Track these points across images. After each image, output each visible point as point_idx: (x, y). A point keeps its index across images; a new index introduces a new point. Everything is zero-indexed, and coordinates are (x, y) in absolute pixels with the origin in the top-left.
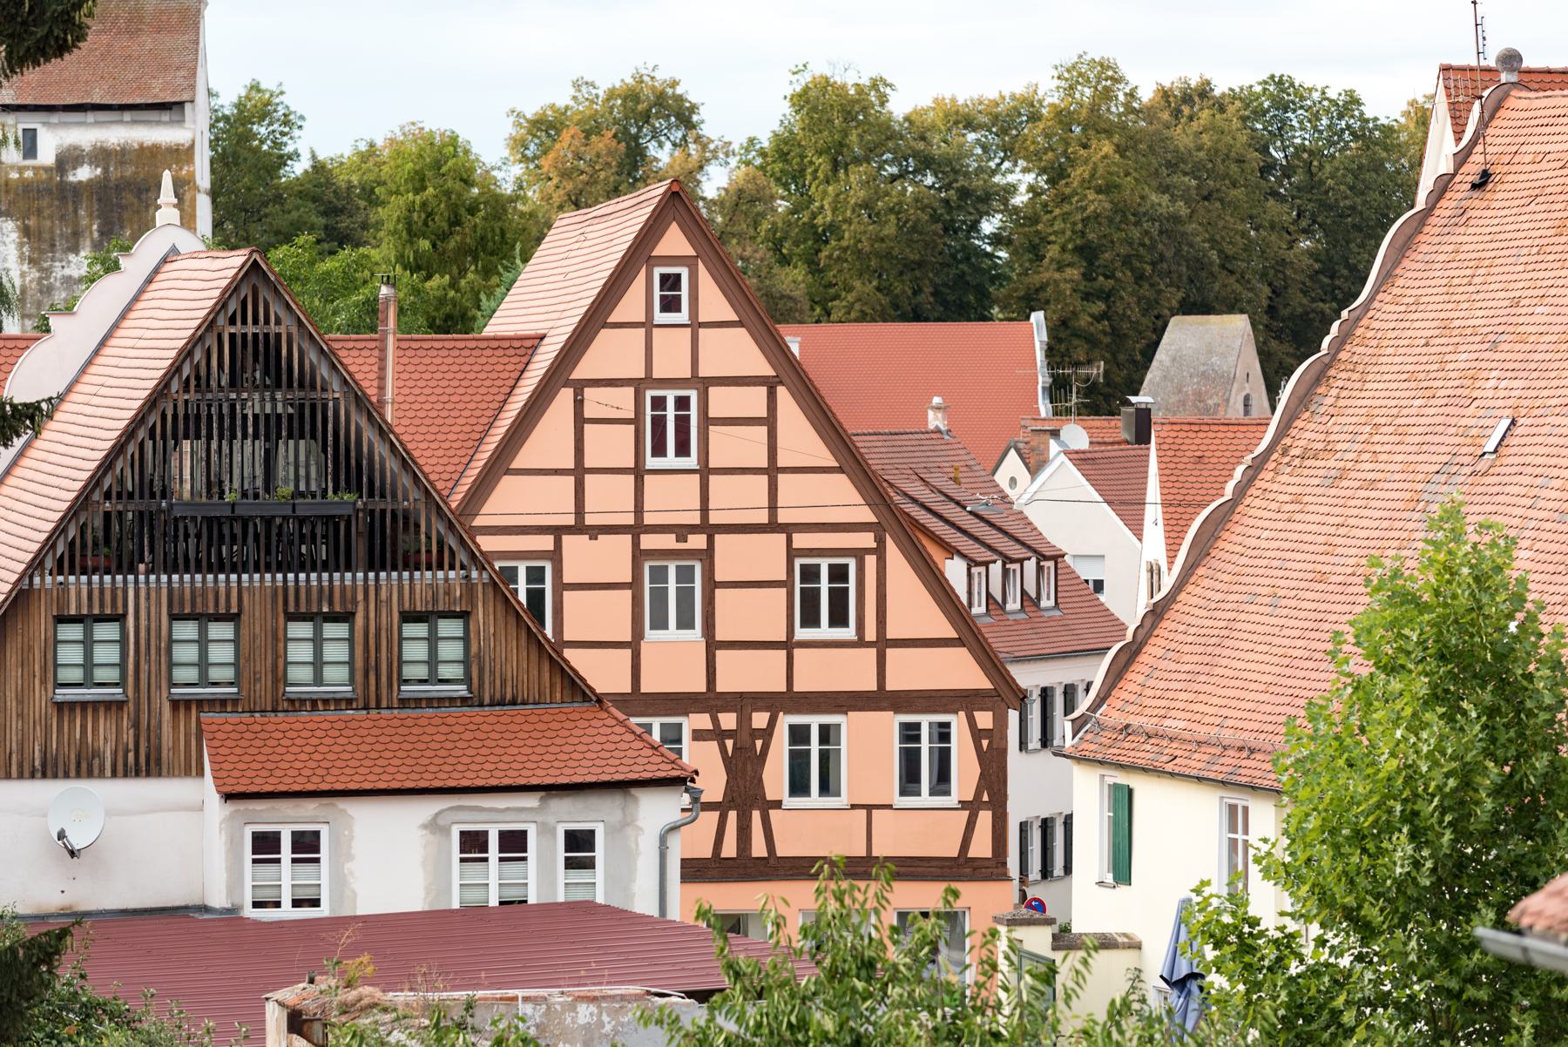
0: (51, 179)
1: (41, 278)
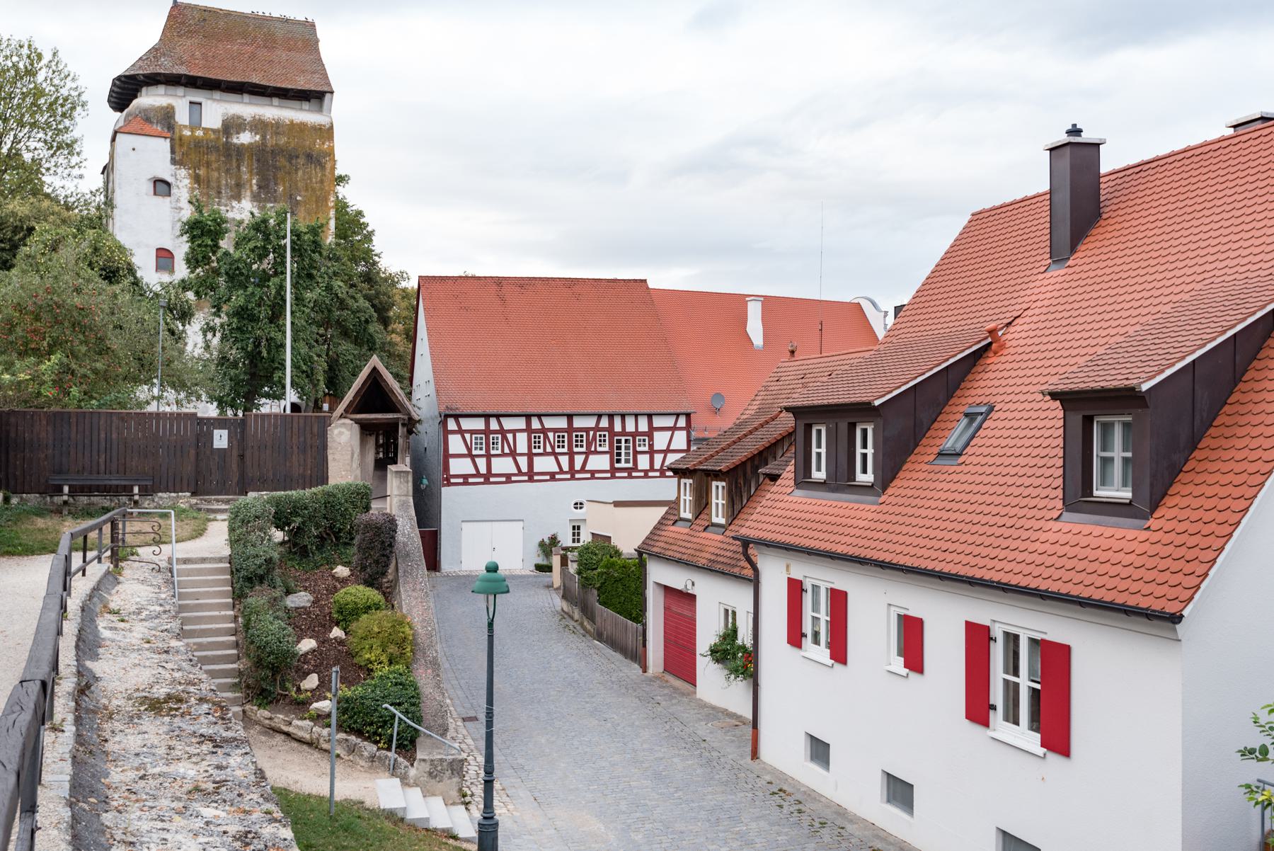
0: (218, 138)
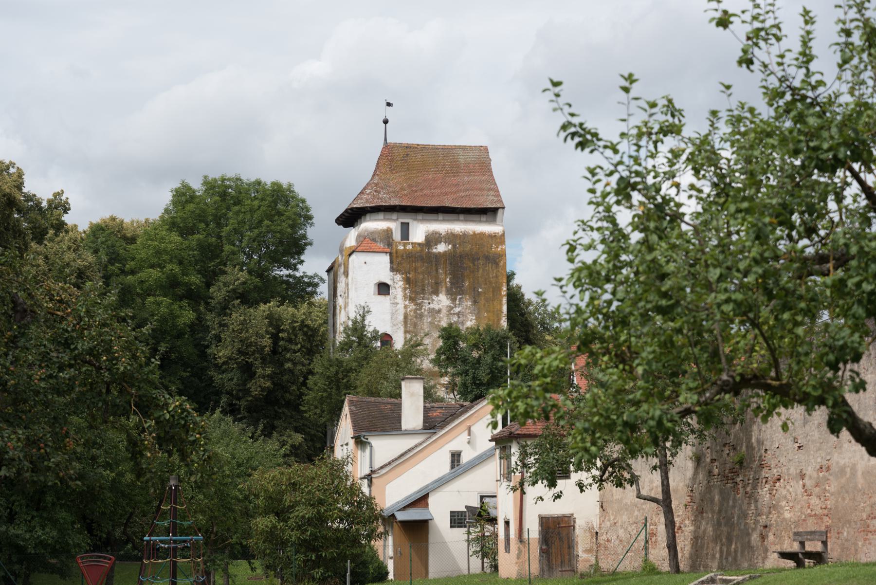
1: (416, 309)
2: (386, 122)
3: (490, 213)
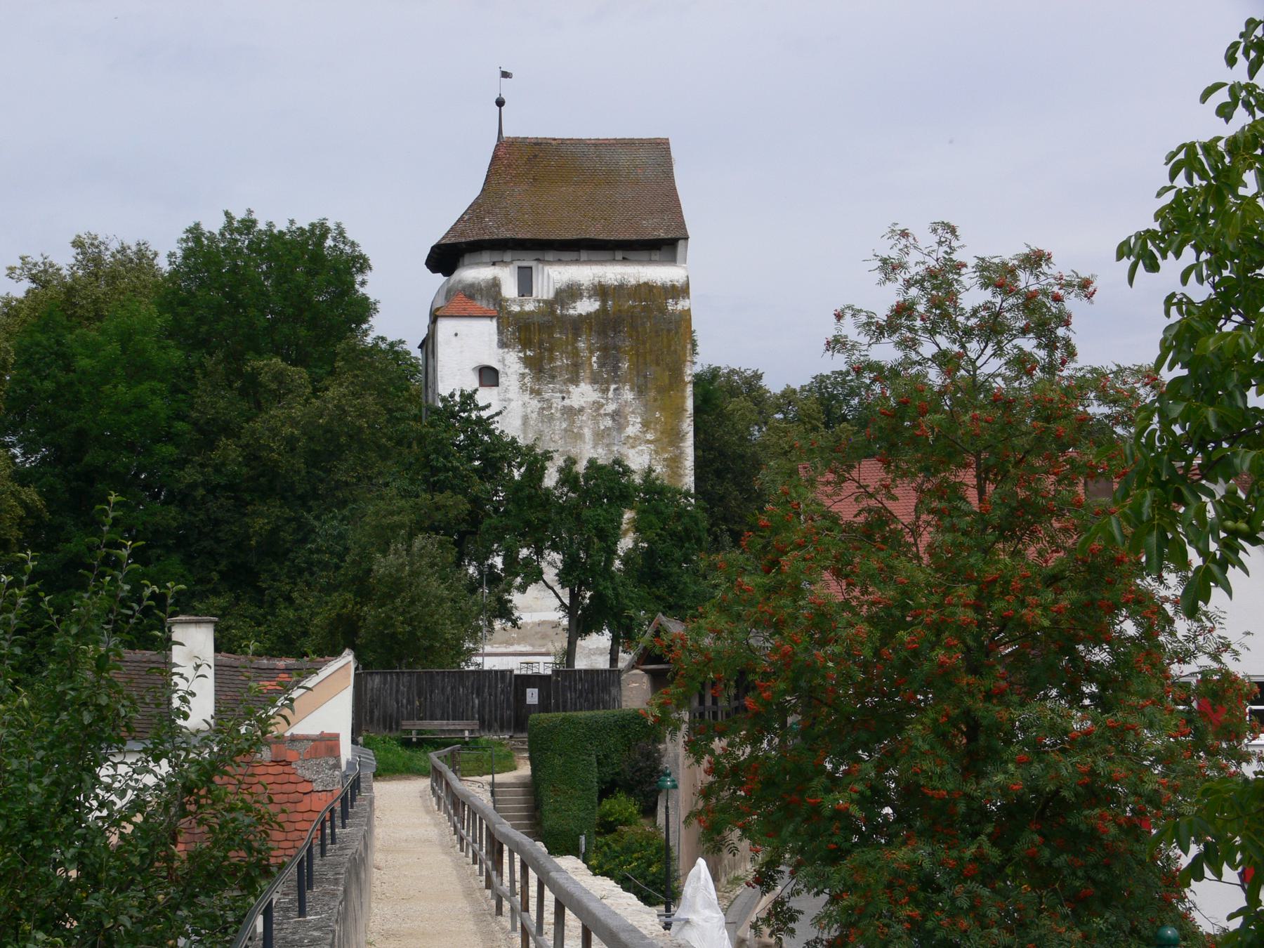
2: (500, 103)
3: (666, 246)
